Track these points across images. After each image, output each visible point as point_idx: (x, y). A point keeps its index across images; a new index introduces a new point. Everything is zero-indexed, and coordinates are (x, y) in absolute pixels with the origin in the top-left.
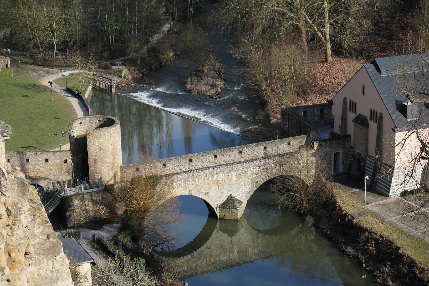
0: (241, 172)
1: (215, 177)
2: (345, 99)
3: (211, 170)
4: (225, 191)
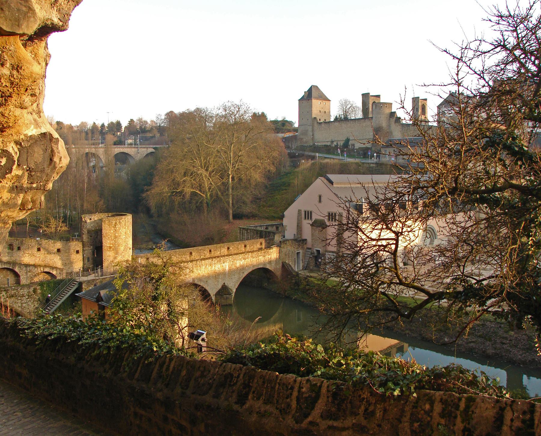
0: (232, 263)
1: (213, 266)
2: (299, 211)
3: (210, 260)
4: (220, 280)
